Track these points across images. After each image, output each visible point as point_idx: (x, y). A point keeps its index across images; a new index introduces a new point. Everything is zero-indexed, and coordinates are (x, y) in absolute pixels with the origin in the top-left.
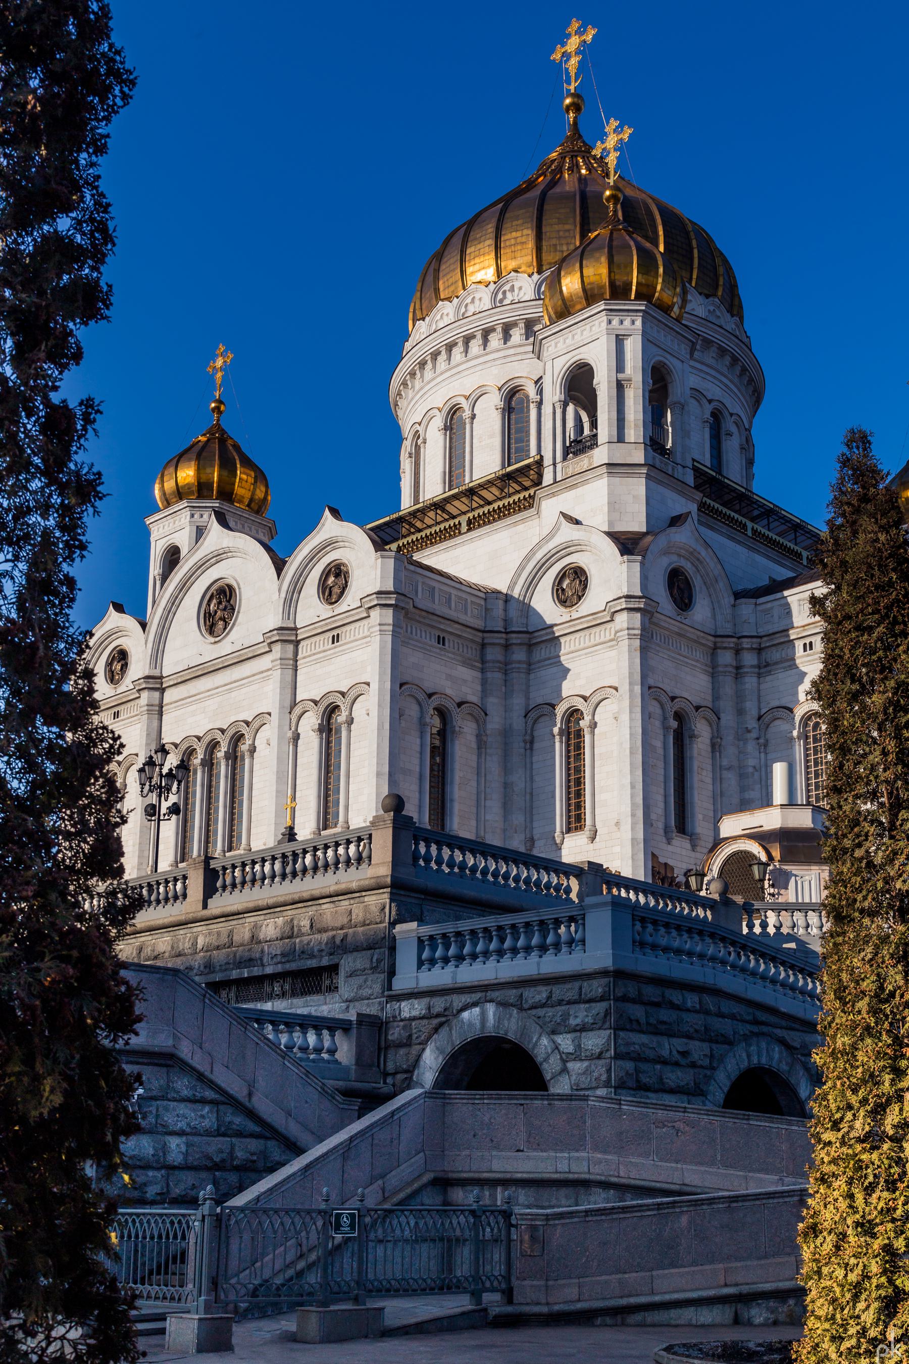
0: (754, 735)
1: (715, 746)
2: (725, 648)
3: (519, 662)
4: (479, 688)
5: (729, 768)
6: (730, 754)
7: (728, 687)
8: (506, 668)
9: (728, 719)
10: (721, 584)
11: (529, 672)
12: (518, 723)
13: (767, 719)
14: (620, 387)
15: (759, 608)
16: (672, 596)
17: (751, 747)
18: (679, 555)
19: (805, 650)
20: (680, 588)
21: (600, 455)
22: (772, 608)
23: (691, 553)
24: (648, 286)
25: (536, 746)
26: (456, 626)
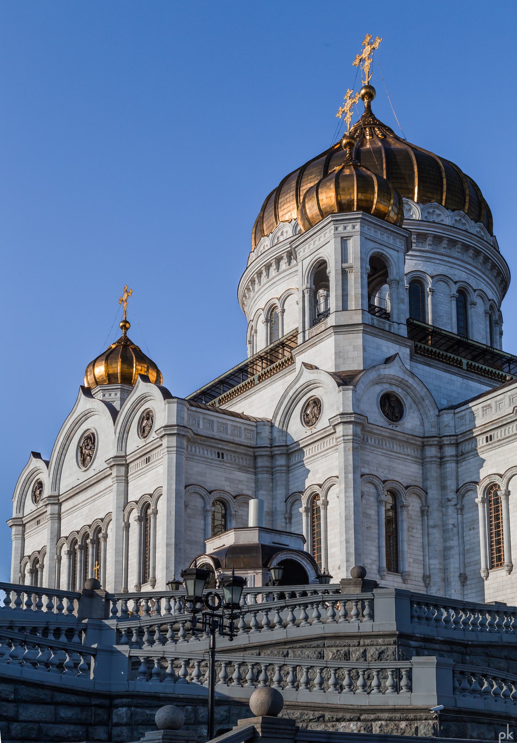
0: (453, 502)
1: (424, 512)
2: (431, 445)
3: (281, 466)
4: (253, 485)
5: (434, 527)
6: (435, 516)
7: (433, 471)
8: (271, 471)
9: (433, 493)
10: (427, 402)
11: (288, 472)
12: (281, 506)
13: (462, 491)
14: (344, 273)
15: (457, 416)
16: (384, 412)
17: (451, 510)
18: (391, 384)
19: (487, 441)
20: (392, 406)
21: (331, 321)
22: (465, 415)
23: (401, 382)
24: (367, 201)
25: (293, 520)
26: (231, 445)
